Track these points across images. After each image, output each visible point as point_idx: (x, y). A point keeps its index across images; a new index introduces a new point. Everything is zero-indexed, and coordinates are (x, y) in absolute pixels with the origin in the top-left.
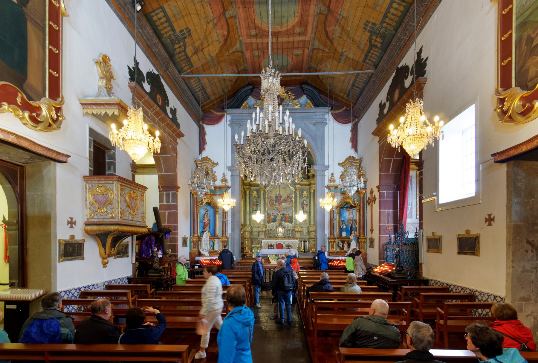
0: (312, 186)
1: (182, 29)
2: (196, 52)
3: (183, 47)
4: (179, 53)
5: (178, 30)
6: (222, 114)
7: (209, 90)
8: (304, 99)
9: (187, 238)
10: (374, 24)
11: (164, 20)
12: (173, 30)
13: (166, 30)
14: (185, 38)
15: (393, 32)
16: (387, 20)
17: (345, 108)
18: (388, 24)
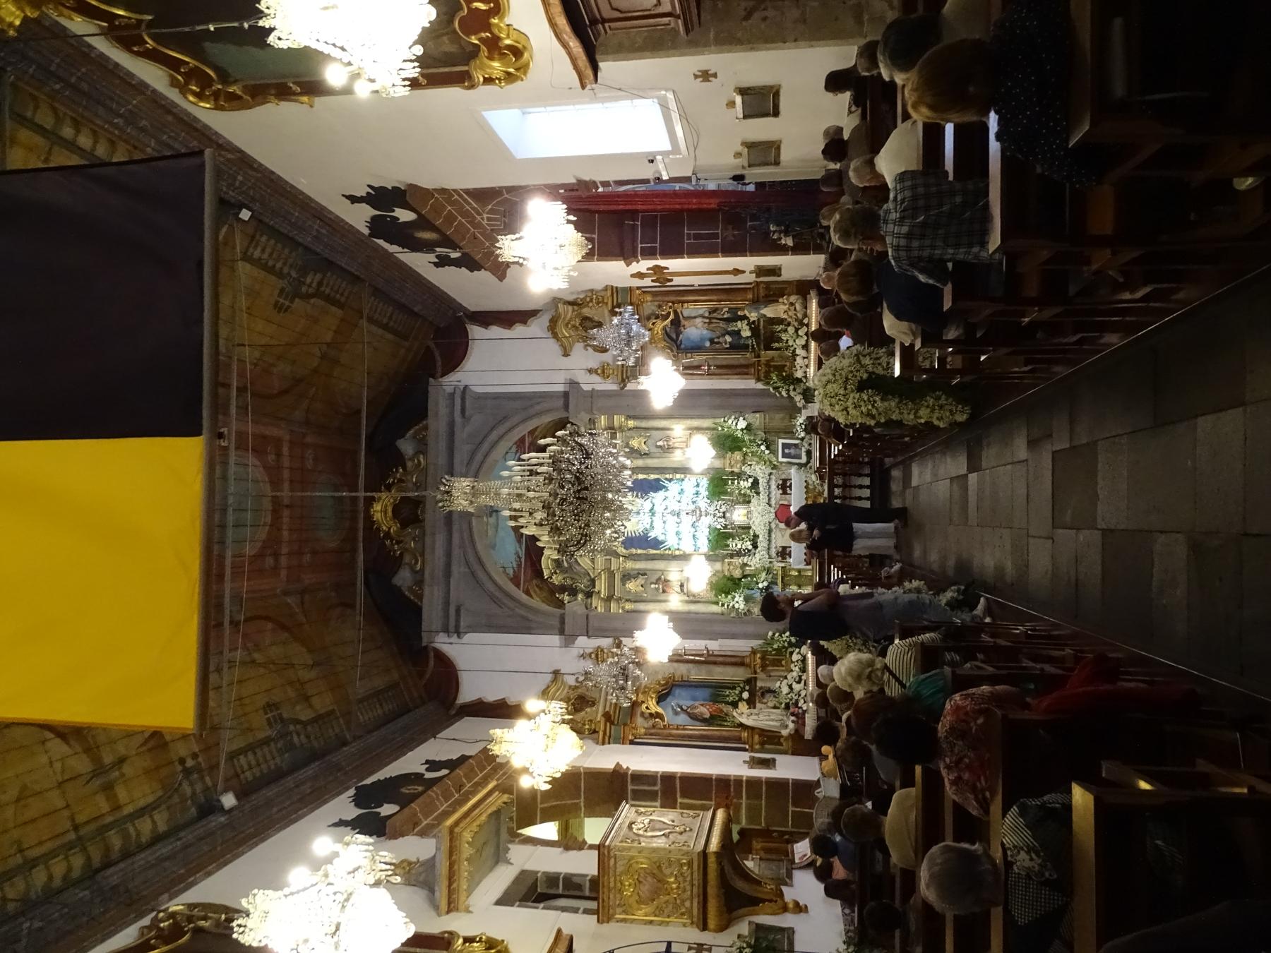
0: (616, 424)
1: (265, 723)
2: (307, 698)
3: (298, 727)
4: (308, 737)
5: (268, 732)
6: (432, 654)
7: (379, 682)
8: (406, 446)
9: (753, 759)
10: (282, 290)
11: (250, 756)
12: (266, 742)
13: (269, 757)
14: (282, 720)
15: (300, 249)
16: (279, 265)
17: (432, 345)
18: (285, 264)
